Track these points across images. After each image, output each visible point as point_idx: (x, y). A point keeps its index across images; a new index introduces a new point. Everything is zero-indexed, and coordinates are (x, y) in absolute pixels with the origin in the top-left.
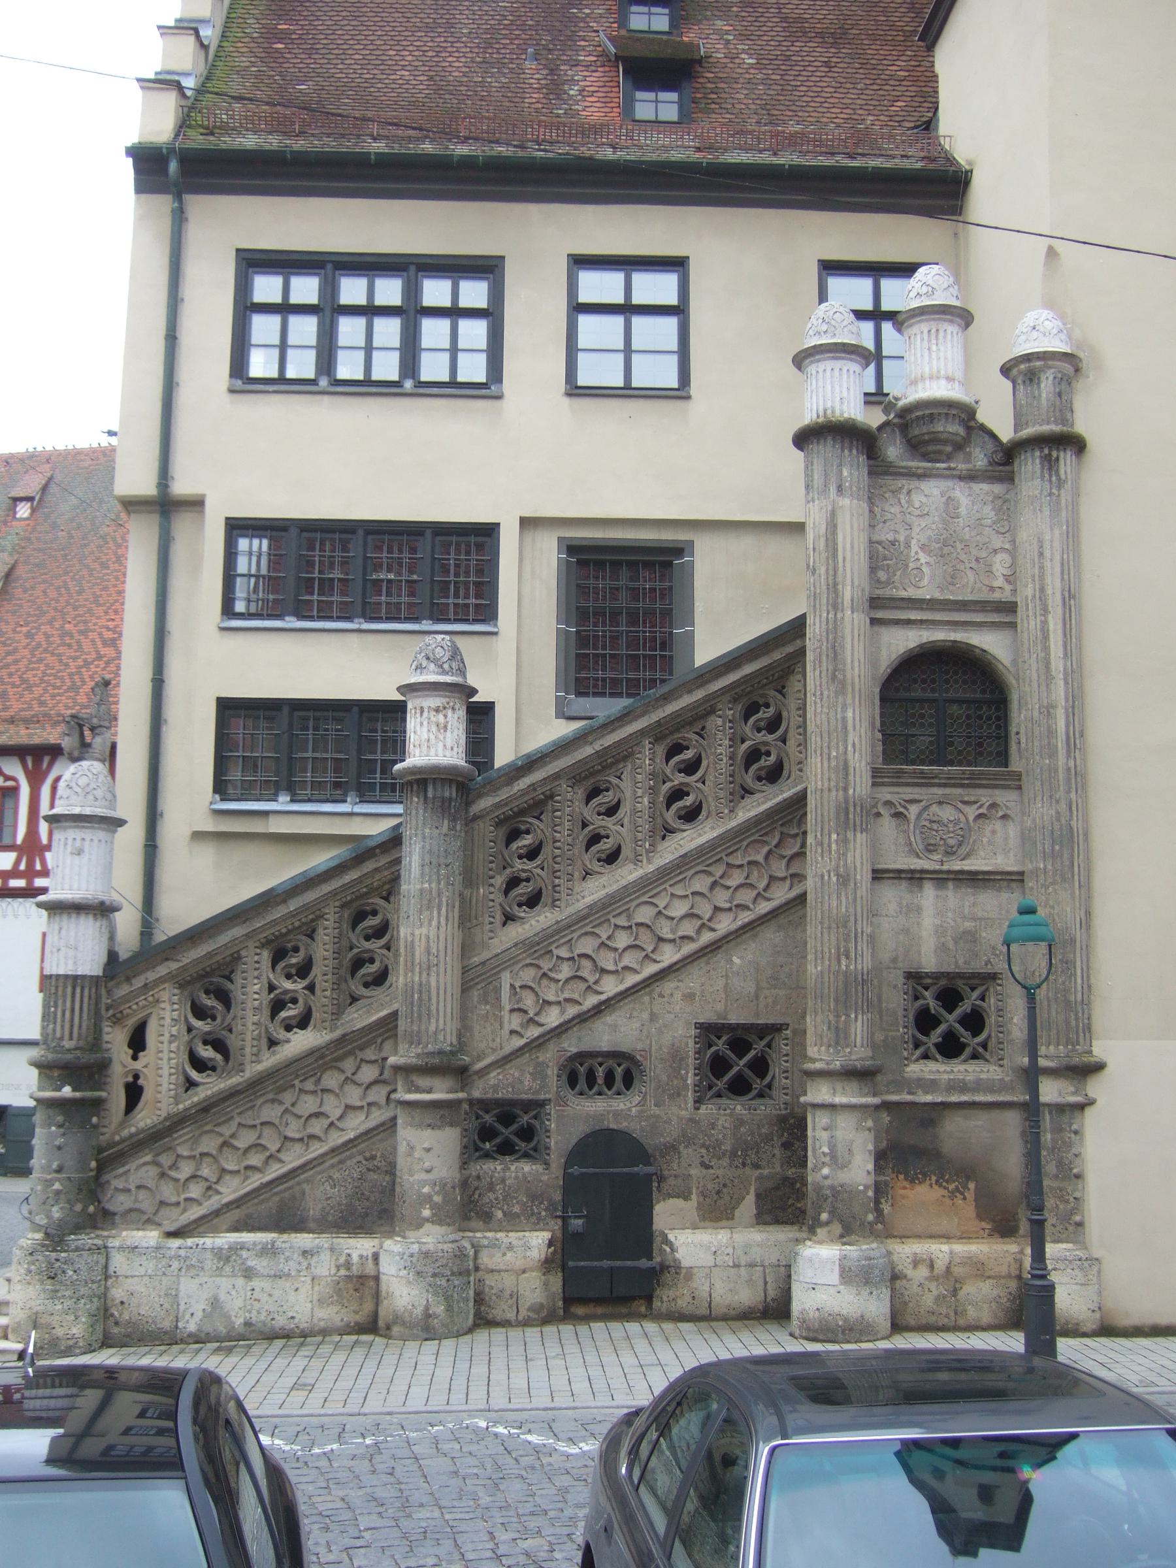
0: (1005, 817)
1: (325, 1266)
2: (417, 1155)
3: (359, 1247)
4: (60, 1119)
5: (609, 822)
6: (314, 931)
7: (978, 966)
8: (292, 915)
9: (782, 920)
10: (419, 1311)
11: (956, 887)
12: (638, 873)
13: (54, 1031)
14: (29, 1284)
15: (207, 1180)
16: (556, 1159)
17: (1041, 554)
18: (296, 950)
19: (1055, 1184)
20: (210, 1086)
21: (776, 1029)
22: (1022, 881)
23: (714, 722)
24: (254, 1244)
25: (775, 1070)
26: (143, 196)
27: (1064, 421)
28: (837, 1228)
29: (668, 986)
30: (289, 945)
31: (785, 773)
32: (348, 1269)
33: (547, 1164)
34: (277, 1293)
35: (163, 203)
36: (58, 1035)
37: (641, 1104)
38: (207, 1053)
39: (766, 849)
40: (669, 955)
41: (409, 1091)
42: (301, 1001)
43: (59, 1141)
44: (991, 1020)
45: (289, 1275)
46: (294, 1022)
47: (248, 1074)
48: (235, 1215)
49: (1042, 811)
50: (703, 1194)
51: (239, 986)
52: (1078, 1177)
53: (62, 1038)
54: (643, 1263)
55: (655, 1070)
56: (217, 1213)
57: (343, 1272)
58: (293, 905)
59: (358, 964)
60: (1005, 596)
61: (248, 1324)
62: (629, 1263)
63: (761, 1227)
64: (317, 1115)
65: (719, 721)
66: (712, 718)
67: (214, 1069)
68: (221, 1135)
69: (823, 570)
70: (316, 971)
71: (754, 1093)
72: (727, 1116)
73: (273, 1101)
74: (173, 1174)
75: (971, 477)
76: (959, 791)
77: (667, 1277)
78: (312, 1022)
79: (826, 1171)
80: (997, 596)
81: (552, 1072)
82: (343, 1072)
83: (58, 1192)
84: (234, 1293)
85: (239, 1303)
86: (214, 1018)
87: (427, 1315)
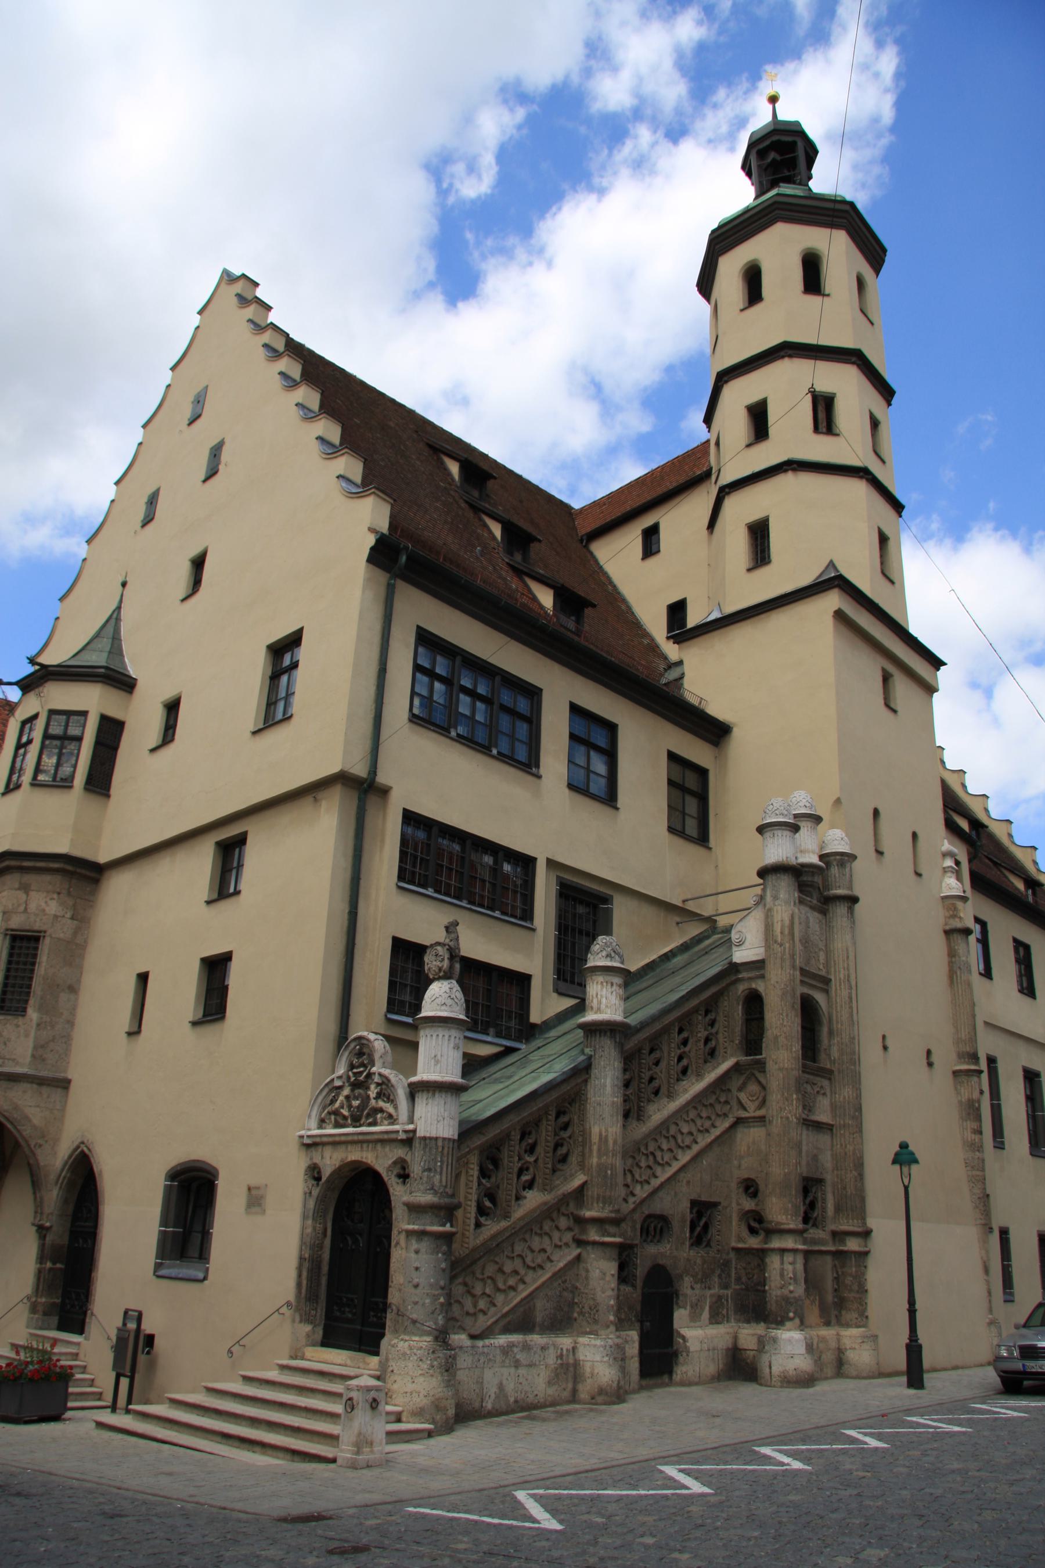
0: (824, 1094)
1: (551, 1359)
2: (607, 1279)
3: (565, 1342)
4: (445, 1248)
5: (657, 1070)
7: (817, 1175)
8: (539, 1109)
11: (808, 1129)
12: (674, 1106)
13: (441, 1181)
14: (432, 1376)
15: (489, 1296)
16: (639, 1283)
17: (848, 957)
18: (530, 1133)
20: (492, 1227)
21: (715, 1205)
22: (831, 1130)
24: (519, 1343)
25: (712, 1231)
26: (371, 566)
27: (851, 888)
28: (797, 1321)
29: (682, 1175)
31: (717, 1053)
32: (561, 1359)
33: (634, 1286)
35: (382, 577)
36: (444, 1183)
37: (670, 1249)
38: (488, 1204)
39: (714, 1097)
40: (684, 1158)
41: (603, 1235)
42: (531, 1169)
43: (443, 1265)
44: (819, 1204)
45: (535, 1365)
46: (527, 1185)
47: (513, 1220)
48: (501, 1324)
49: (846, 1093)
50: (692, 1307)
55: (675, 1224)
56: (496, 1322)
57: (559, 1361)
58: (540, 1104)
59: (558, 1145)
60: (823, 973)
61: (516, 1401)
63: (715, 1326)
64: (539, 1252)
65: (700, 1018)
67: (487, 1215)
68: (497, 1263)
69: (787, 945)
70: (540, 1150)
71: (704, 1244)
72: (696, 1255)
73: (520, 1240)
74: (473, 1291)
75: (813, 908)
76: (811, 1077)
77: (681, 1359)
78: (536, 1185)
79: (791, 1288)
80: (820, 973)
81: (638, 1226)
82: (553, 1220)
83: (442, 1304)
85: (512, 1386)
87: (619, 1387)
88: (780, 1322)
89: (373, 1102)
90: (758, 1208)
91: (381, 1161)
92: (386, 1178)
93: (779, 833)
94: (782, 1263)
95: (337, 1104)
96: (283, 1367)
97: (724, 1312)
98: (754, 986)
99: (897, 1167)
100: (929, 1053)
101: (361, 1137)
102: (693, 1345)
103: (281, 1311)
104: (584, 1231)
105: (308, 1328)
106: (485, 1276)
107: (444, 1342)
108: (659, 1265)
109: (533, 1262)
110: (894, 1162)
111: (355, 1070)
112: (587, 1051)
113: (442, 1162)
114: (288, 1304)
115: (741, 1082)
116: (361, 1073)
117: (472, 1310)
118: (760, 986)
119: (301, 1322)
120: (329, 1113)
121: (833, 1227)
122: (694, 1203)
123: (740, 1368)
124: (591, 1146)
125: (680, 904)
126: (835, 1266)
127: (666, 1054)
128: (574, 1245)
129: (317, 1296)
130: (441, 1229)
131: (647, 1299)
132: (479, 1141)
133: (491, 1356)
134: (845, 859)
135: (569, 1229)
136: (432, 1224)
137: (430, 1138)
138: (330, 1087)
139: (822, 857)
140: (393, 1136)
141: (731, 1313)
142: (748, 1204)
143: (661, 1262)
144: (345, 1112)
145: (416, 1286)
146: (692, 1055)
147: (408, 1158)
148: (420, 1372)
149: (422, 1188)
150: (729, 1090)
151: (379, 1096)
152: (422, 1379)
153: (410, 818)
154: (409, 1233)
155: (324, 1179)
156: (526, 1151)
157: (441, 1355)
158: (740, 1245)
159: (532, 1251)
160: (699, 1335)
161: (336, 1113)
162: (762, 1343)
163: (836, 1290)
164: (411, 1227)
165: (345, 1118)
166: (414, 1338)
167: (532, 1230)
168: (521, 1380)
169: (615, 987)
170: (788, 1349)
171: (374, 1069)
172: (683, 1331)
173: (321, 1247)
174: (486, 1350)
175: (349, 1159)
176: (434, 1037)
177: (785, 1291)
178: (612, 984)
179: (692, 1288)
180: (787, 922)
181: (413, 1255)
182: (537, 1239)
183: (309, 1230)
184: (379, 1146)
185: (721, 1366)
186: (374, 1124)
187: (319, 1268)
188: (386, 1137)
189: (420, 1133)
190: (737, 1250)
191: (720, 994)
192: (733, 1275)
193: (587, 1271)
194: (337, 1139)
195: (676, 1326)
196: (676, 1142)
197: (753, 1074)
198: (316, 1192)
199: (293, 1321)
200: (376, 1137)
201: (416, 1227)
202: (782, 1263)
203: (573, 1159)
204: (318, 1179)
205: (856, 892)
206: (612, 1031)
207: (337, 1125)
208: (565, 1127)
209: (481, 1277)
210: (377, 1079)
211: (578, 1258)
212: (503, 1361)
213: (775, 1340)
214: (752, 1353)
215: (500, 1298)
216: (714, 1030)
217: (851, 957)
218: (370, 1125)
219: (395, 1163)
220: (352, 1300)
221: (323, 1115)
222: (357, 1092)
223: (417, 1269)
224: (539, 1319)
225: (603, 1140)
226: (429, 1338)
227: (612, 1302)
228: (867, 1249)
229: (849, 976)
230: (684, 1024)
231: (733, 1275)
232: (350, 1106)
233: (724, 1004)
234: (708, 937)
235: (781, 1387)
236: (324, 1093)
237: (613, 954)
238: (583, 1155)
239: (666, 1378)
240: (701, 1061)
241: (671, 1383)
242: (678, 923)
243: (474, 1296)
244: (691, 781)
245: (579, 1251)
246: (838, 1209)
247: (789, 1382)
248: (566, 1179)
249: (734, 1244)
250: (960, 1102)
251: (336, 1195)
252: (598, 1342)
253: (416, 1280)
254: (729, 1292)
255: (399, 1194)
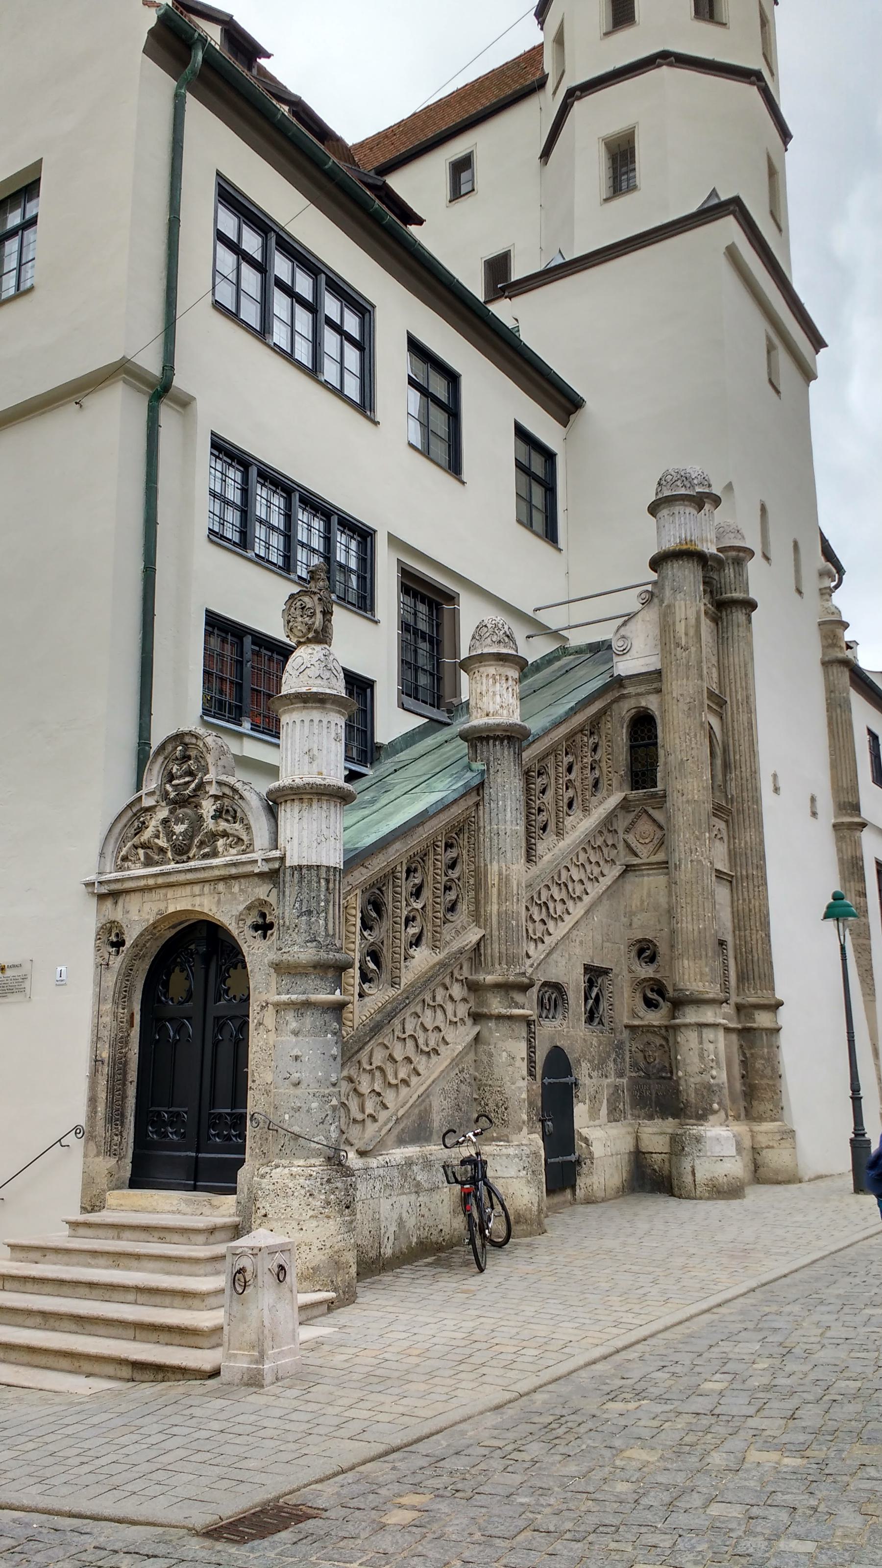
6: (425, 855)
9: (609, 892)
10: (535, 1208)
14: (328, 1217)
15: (379, 1094)
17: (746, 675)
18: (415, 870)
19: (771, 1083)
21: (605, 972)
23: (578, 737)
25: (604, 1005)
27: (747, 591)
28: (722, 1114)
29: (575, 932)
30: (413, 865)
31: (600, 785)
34: (433, 1206)
36: (331, 933)
38: (372, 965)
41: (510, 1007)
42: (418, 918)
43: (335, 1051)
49: (748, 836)
51: (390, 899)
52: (780, 1077)
53: (334, 935)
54: (573, 1158)
62: (568, 1158)
66: (580, 735)
68: (387, 1048)
69: (693, 649)
70: (427, 893)
77: (585, 1169)
79: (714, 1073)
83: (334, 1109)
84: (410, 1211)
86: (371, 929)
88: (702, 1117)
89: (210, 824)
90: (658, 976)
91: (226, 909)
92: (235, 932)
93: (681, 509)
94: (701, 1043)
95: (147, 835)
96: (74, 1225)
97: (621, 1106)
98: (643, 704)
99: (831, 923)
100: (813, 799)
101: (190, 876)
102: (598, 1150)
103: (64, 1142)
104: (482, 1003)
105: (113, 1161)
106: (374, 1066)
107: (340, 1164)
108: (557, 1047)
109: (427, 1045)
110: (826, 916)
111: (175, 782)
112: (478, 766)
113: (327, 902)
114: (77, 1130)
115: (626, 823)
116: (187, 783)
117: (360, 1117)
118: (651, 703)
119: (98, 1155)
120: (136, 847)
121: (739, 1000)
122: (588, 969)
123: (652, 1179)
124: (486, 893)
125: (531, 613)
126: (741, 1046)
127: (553, 781)
128: (469, 1022)
129: (123, 1115)
130: (331, 997)
131: (548, 1092)
132: (361, 876)
133: (388, 1181)
134: (740, 556)
135: (464, 1000)
136: (316, 990)
137: (309, 867)
138: (135, 810)
139: (719, 550)
140: (248, 869)
141: (628, 1107)
142: (646, 972)
143: (558, 1044)
144: (162, 842)
145: (297, 1084)
146: (577, 784)
147: (272, 899)
148: (311, 1213)
149: (299, 940)
150: (616, 831)
151: (218, 815)
152: (315, 1223)
153: (221, 448)
154: (279, 1007)
155: (128, 944)
156: (412, 894)
157: (339, 1185)
158: (636, 1022)
159: (426, 1030)
160: (604, 1138)
161: (143, 846)
162: (678, 1146)
163: (743, 1077)
164: (284, 997)
165: (162, 850)
166: (296, 1162)
167: (424, 1001)
168: (424, 1210)
169: (510, 682)
170: (717, 1150)
171: (207, 778)
172: (584, 1132)
173: (124, 1041)
174: (381, 1171)
175: (171, 909)
176: (307, 723)
177: (706, 1077)
178: (507, 679)
179: (591, 1077)
180: (692, 621)
181: (293, 1039)
182: (429, 1012)
183: (107, 1019)
184: (221, 887)
185: (625, 1175)
186: (215, 854)
187: (125, 1074)
188: (233, 871)
189: (292, 860)
190: (632, 1028)
191: (603, 712)
192: (628, 1059)
193: (491, 1055)
194: (151, 882)
195: (576, 1126)
196: (568, 892)
197: (646, 812)
198: (117, 962)
199: (85, 1156)
200: (217, 873)
201: (294, 997)
202: (701, 1043)
203: (463, 907)
204: (118, 944)
205: (752, 595)
206: (509, 738)
207: (149, 862)
208: (452, 865)
209: (368, 1068)
210: (213, 790)
211: (477, 1039)
212: (402, 1186)
213: (698, 1139)
214: (660, 1157)
215: (389, 1097)
216: (597, 757)
217: (750, 675)
218: (205, 856)
219: (249, 908)
220: (178, 1114)
221: (123, 853)
222: (180, 812)
223: (297, 1058)
224: (436, 1124)
225: (505, 880)
226: (318, 1161)
227: (524, 1096)
228: (776, 1027)
229: (748, 697)
230: (570, 743)
231: (628, 1059)
232: (170, 834)
233: (607, 727)
234: (558, 658)
235: (709, 1199)
236: (124, 820)
237: (506, 639)
238: (477, 902)
239: (568, 1193)
240: (588, 793)
241: (574, 1201)
242: (528, 637)
243: (361, 1095)
244: (538, 465)
245: (477, 1029)
246: (742, 978)
247: (719, 1192)
248: (458, 932)
249: (626, 1021)
250: (841, 861)
251: (146, 965)
252: (511, 1151)
253: (298, 1075)
254: (625, 1081)
255: (257, 953)
